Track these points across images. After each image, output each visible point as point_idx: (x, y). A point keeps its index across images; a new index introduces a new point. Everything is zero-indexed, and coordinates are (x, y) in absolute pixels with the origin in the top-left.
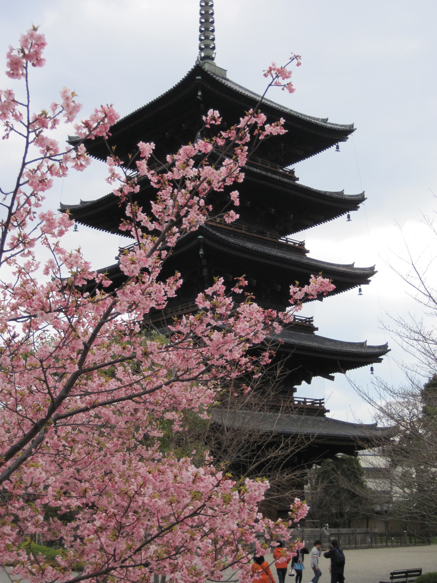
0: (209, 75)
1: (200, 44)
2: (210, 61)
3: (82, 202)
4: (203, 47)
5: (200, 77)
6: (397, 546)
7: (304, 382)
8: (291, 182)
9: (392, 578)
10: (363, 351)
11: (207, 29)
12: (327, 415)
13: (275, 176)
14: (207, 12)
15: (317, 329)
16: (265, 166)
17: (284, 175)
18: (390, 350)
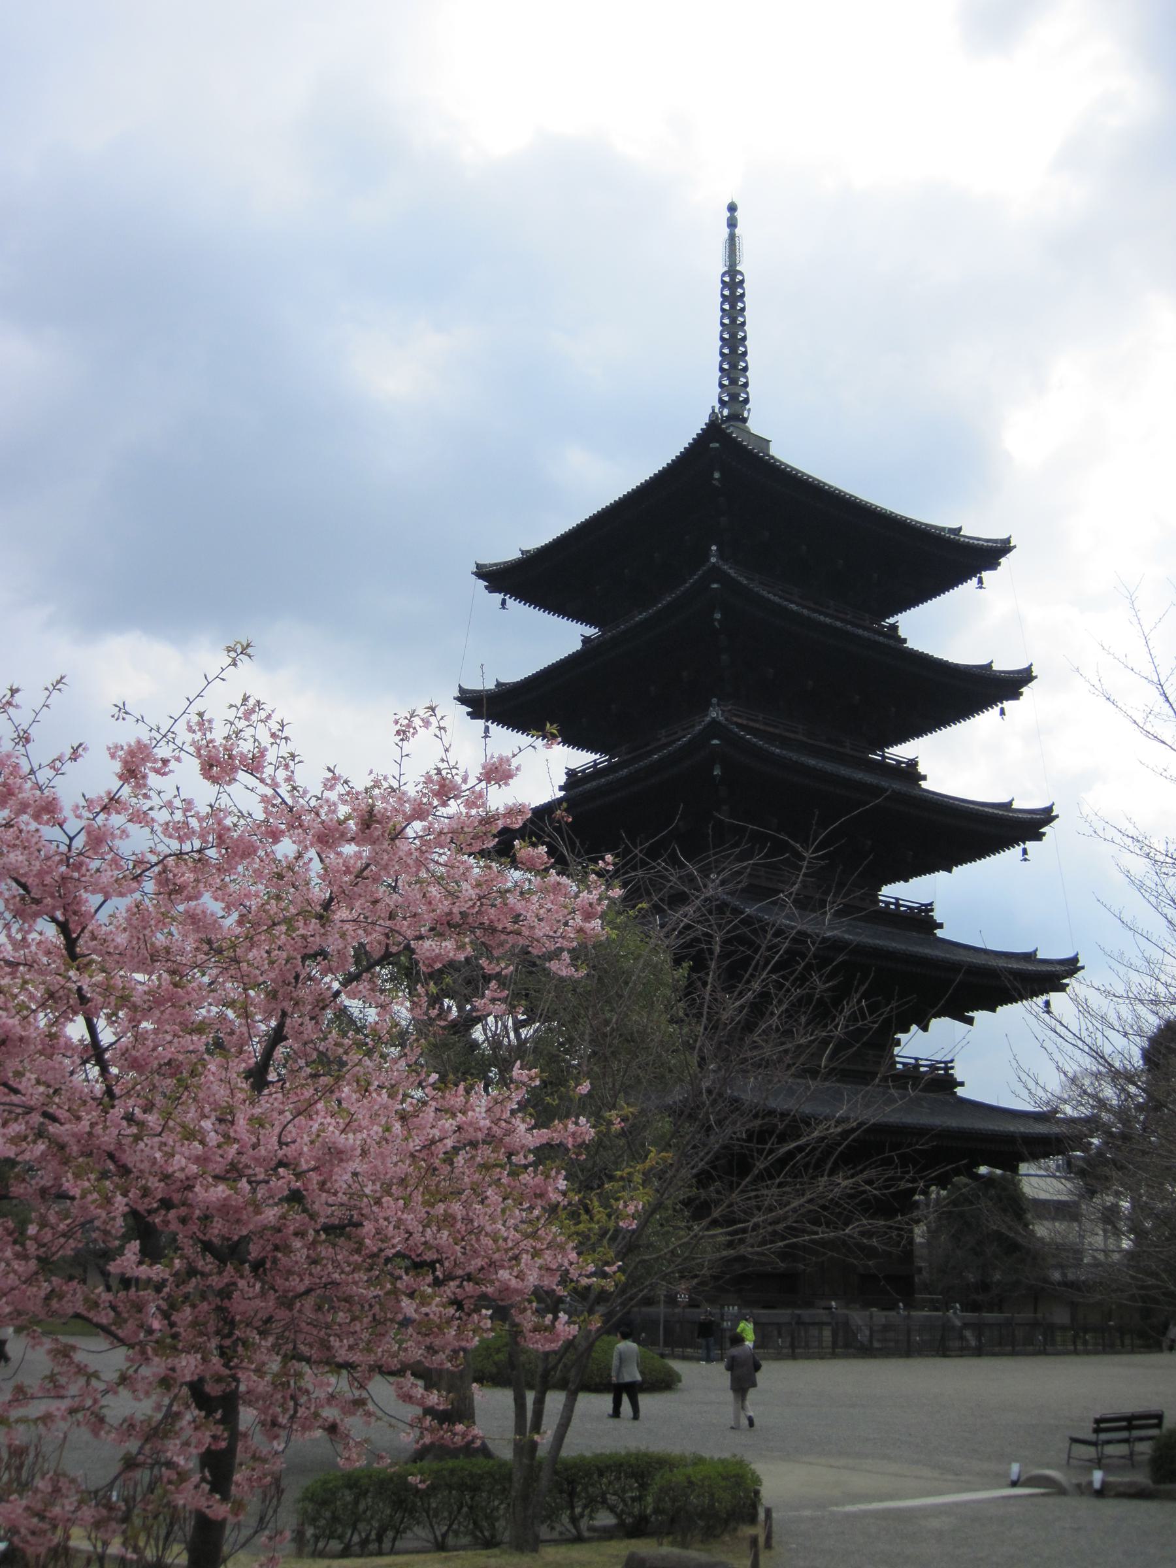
0: (735, 439)
1: (720, 394)
2: (740, 424)
3: (499, 684)
4: (726, 399)
5: (717, 445)
6: (1096, 1353)
7: (914, 1028)
8: (892, 642)
9: (1097, 1431)
10: (1031, 967)
11: (734, 366)
12: (960, 1091)
13: (860, 632)
14: (733, 335)
15: (940, 926)
16: (841, 615)
17: (880, 633)
18: (1083, 968)
